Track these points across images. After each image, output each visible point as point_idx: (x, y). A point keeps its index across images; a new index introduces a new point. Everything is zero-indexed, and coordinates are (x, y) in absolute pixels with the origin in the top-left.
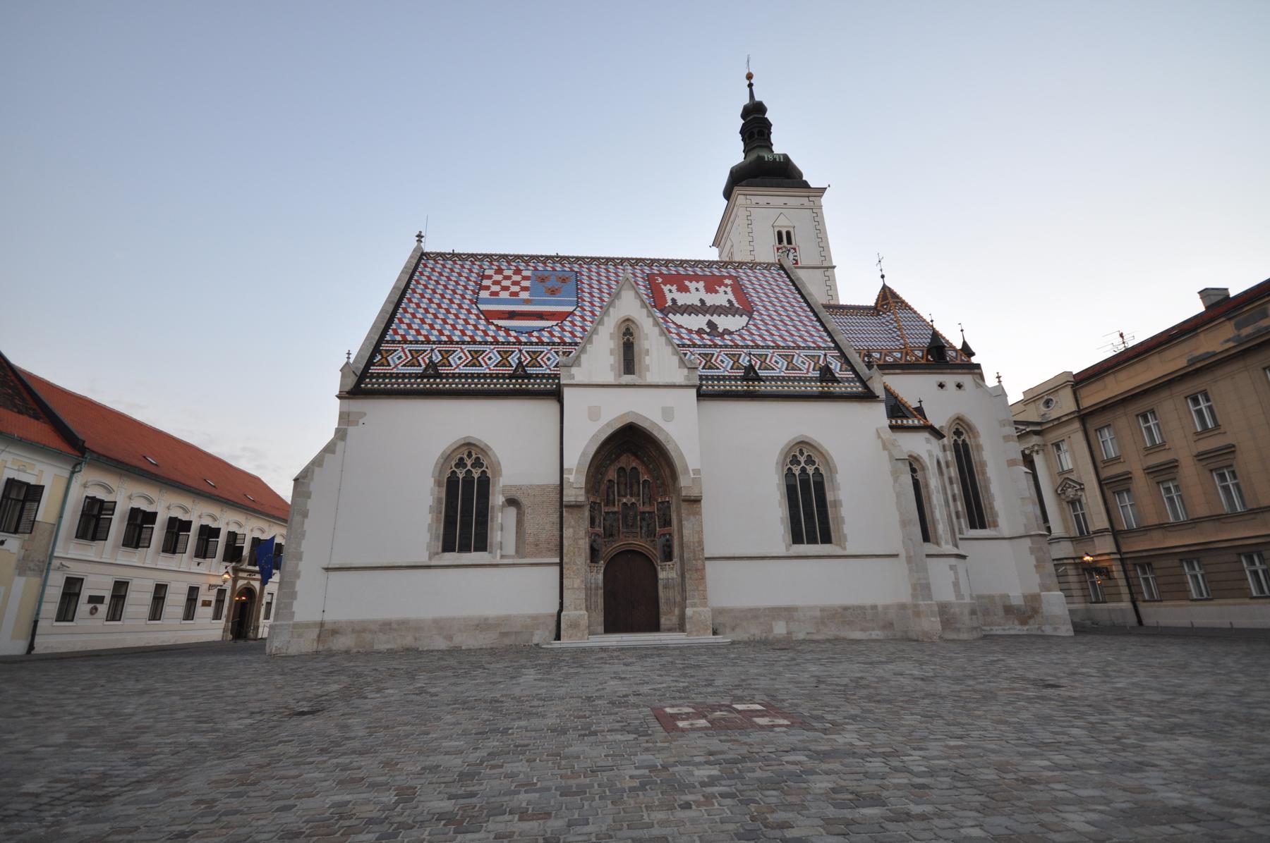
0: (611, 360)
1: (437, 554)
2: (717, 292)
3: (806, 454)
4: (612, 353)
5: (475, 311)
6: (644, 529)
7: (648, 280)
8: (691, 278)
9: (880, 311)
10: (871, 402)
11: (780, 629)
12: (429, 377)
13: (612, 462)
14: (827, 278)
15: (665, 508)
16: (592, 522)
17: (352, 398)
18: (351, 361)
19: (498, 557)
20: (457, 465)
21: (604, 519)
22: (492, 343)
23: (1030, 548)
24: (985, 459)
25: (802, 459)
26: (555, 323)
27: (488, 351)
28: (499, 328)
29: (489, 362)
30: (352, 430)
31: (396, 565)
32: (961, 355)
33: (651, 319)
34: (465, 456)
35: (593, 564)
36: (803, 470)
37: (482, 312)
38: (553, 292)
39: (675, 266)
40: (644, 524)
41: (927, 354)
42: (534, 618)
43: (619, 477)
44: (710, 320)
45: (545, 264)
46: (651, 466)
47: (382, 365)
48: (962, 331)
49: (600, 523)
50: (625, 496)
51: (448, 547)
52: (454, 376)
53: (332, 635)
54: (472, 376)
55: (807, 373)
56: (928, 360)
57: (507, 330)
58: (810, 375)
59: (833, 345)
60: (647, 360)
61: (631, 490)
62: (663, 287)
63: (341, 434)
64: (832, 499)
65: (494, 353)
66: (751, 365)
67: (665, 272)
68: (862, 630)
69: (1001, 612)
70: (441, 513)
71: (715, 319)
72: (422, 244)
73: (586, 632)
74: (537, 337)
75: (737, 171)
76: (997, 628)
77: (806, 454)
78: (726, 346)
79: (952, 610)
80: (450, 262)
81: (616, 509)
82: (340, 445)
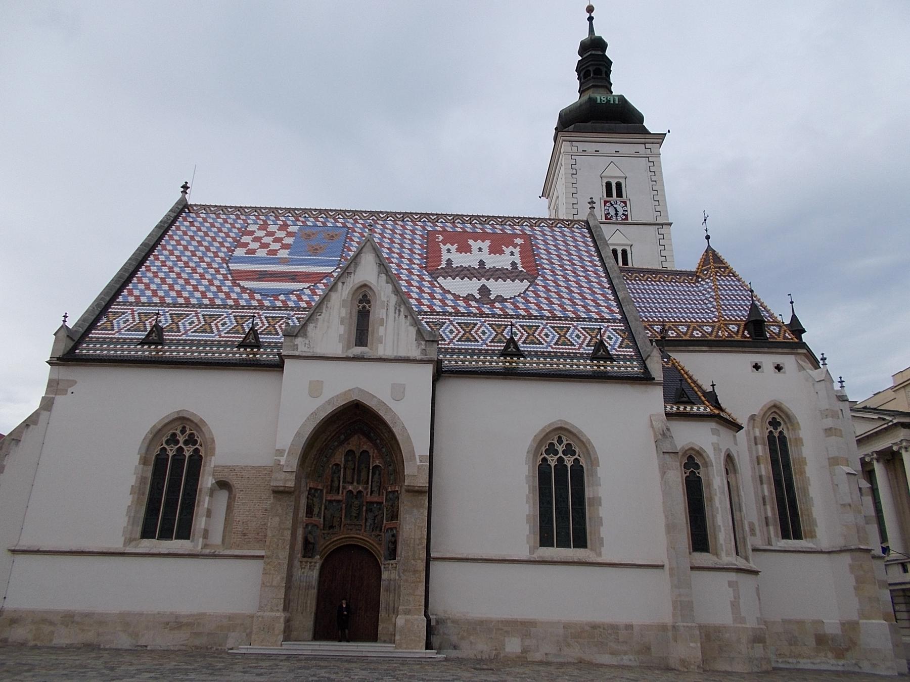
0: (341, 329)
1: (135, 539)
2: (502, 252)
3: (565, 442)
4: (342, 323)
5: (223, 271)
6: (370, 522)
7: (427, 239)
8: (476, 236)
9: (698, 277)
10: (645, 384)
11: (513, 646)
12: (150, 344)
13: (342, 443)
14: (661, 237)
15: (394, 498)
16: (309, 511)
17: (63, 365)
18: (70, 324)
19: (200, 548)
20: (167, 442)
21: (326, 508)
22: (231, 307)
23: (850, 565)
24: (804, 455)
25: (560, 448)
26: (308, 285)
27: (225, 315)
28: (244, 289)
29: (221, 328)
30: (59, 400)
31: (87, 550)
32: (785, 331)
33: (390, 286)
34: (178, 432)
35: (305, 560)
36: (560, 460)
38: (315, 251)
39: (464, 223)
40: (370, 515)
41: (745, 329)
42: (231, 617)
43: (346, 461)
44: (484, 285)
45: (316, 218)
46: (384, 450)
48: (792, 303)
49: (319, 512)
50: (352, 483)
51: (147, 533)
52: (178, 343)
53: (10, 625)
54: (199, 343)
55: (579, 349)
56: (744, 336)
57: (252, 292)
58: (582, 351)
59: (619, 317)
60: (381, 330)
61: (359, 476)
62: (442, 246)
63: (47, 404)
64: (591, 496)
65: (230, 319)
66: (512, 338)
67: (449, 229)
68: (613, 653)
69: (812, 642)
70: (143, 494)
71: (491, 284)
72: (187, 196)
73: (281, 637)
74: (282, 301)
76: (805, 660)
77: (565, 442)
78: (494, 315)
79: (727, 635)
80: (213, 216)
81: (339, 497)
82: (45, 414)
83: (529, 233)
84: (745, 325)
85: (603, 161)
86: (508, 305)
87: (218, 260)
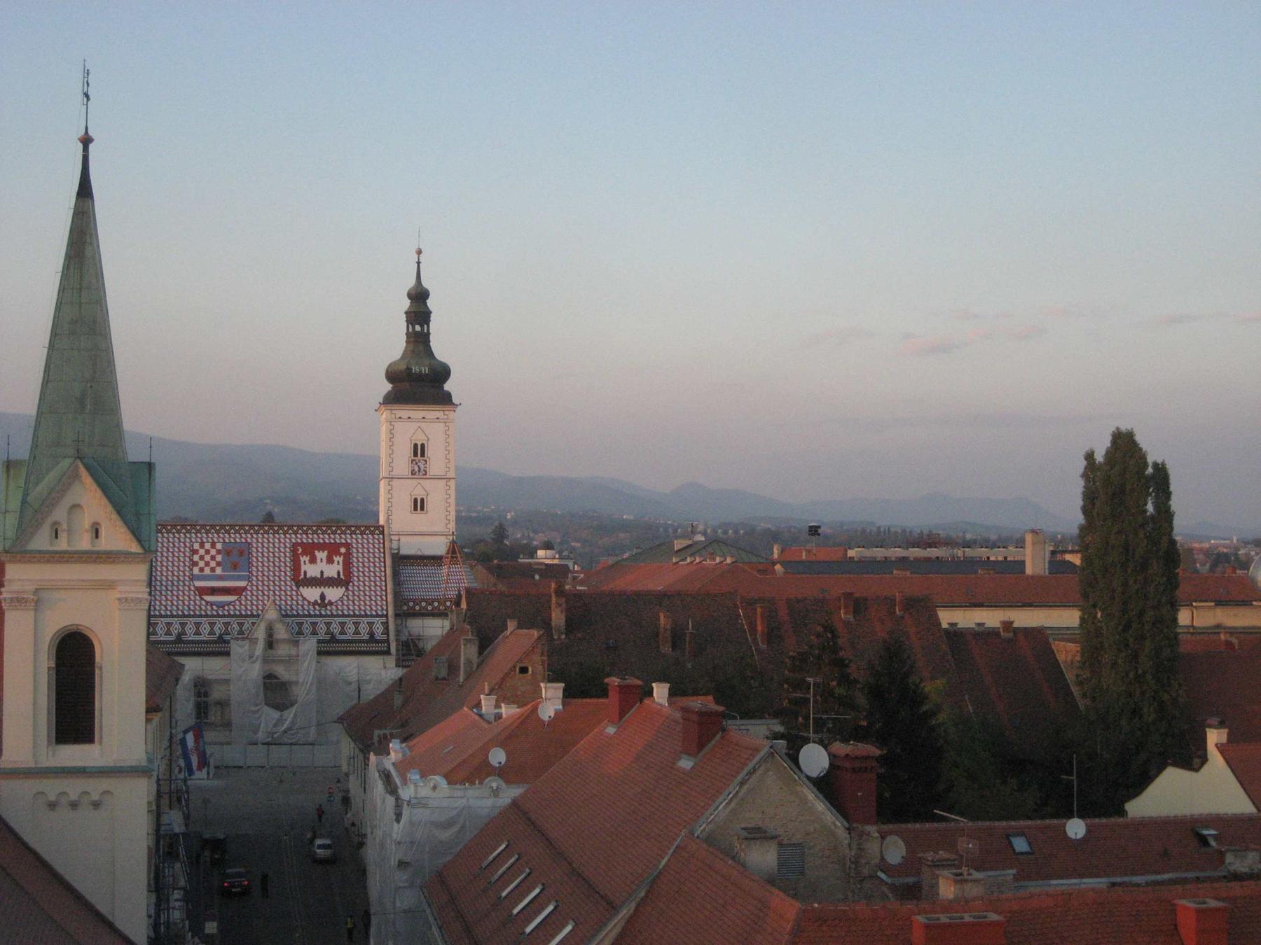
5: (192, 588)
7: (292, 551)
12: (178, 644)
28: (207, 603)
37: (197, 588)
38: (235, 567)
39: (313, 534)
47: (154, 635)
57: (212, 604)
58: (364, 638)
62: (301, 558)
67: (305, 541)
75: (391, 372)
78: (327, 616)
83: (349, 541)
84: (455, 602)
85: (414, 426)
86: (334, 608)
87: (187, 578)
